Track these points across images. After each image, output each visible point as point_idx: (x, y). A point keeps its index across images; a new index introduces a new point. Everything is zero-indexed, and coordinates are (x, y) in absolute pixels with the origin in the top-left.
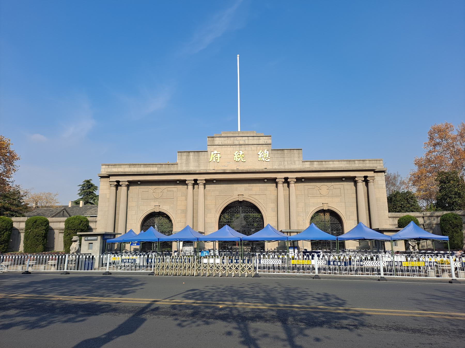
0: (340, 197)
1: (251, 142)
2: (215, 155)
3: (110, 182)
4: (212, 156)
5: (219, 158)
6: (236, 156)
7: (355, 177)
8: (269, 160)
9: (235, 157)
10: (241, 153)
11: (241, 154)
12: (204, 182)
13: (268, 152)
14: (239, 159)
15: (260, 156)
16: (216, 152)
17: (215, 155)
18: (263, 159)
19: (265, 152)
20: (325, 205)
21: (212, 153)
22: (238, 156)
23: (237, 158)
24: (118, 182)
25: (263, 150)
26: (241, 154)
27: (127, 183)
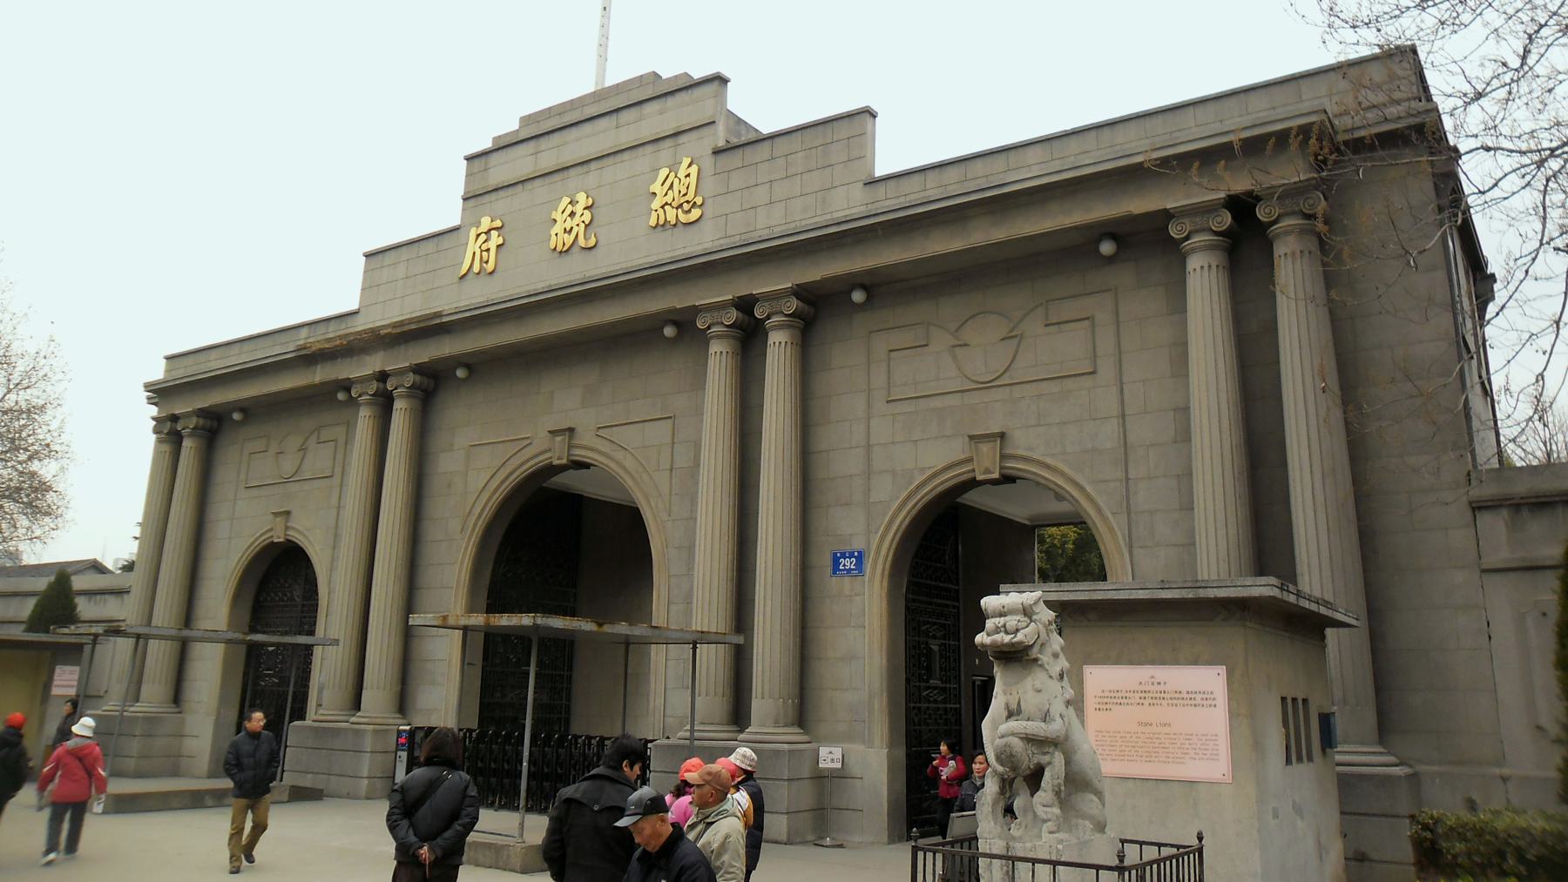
0: (1087, 382)
1: (626, 137)
2: (483, 237)
4: (473, 247)
6: (558, 228)
7: (1167, 215)
8: (696, 213)
10: (582, 199)
11: (579, 209)
13: (694, 170)
14: (569, 239)
16: (486, 223)
17: (483, 237)
18: (671, 214)
20: (985, 448)
21: (473, 233)
25: (674, 168)
26: (579, 209)
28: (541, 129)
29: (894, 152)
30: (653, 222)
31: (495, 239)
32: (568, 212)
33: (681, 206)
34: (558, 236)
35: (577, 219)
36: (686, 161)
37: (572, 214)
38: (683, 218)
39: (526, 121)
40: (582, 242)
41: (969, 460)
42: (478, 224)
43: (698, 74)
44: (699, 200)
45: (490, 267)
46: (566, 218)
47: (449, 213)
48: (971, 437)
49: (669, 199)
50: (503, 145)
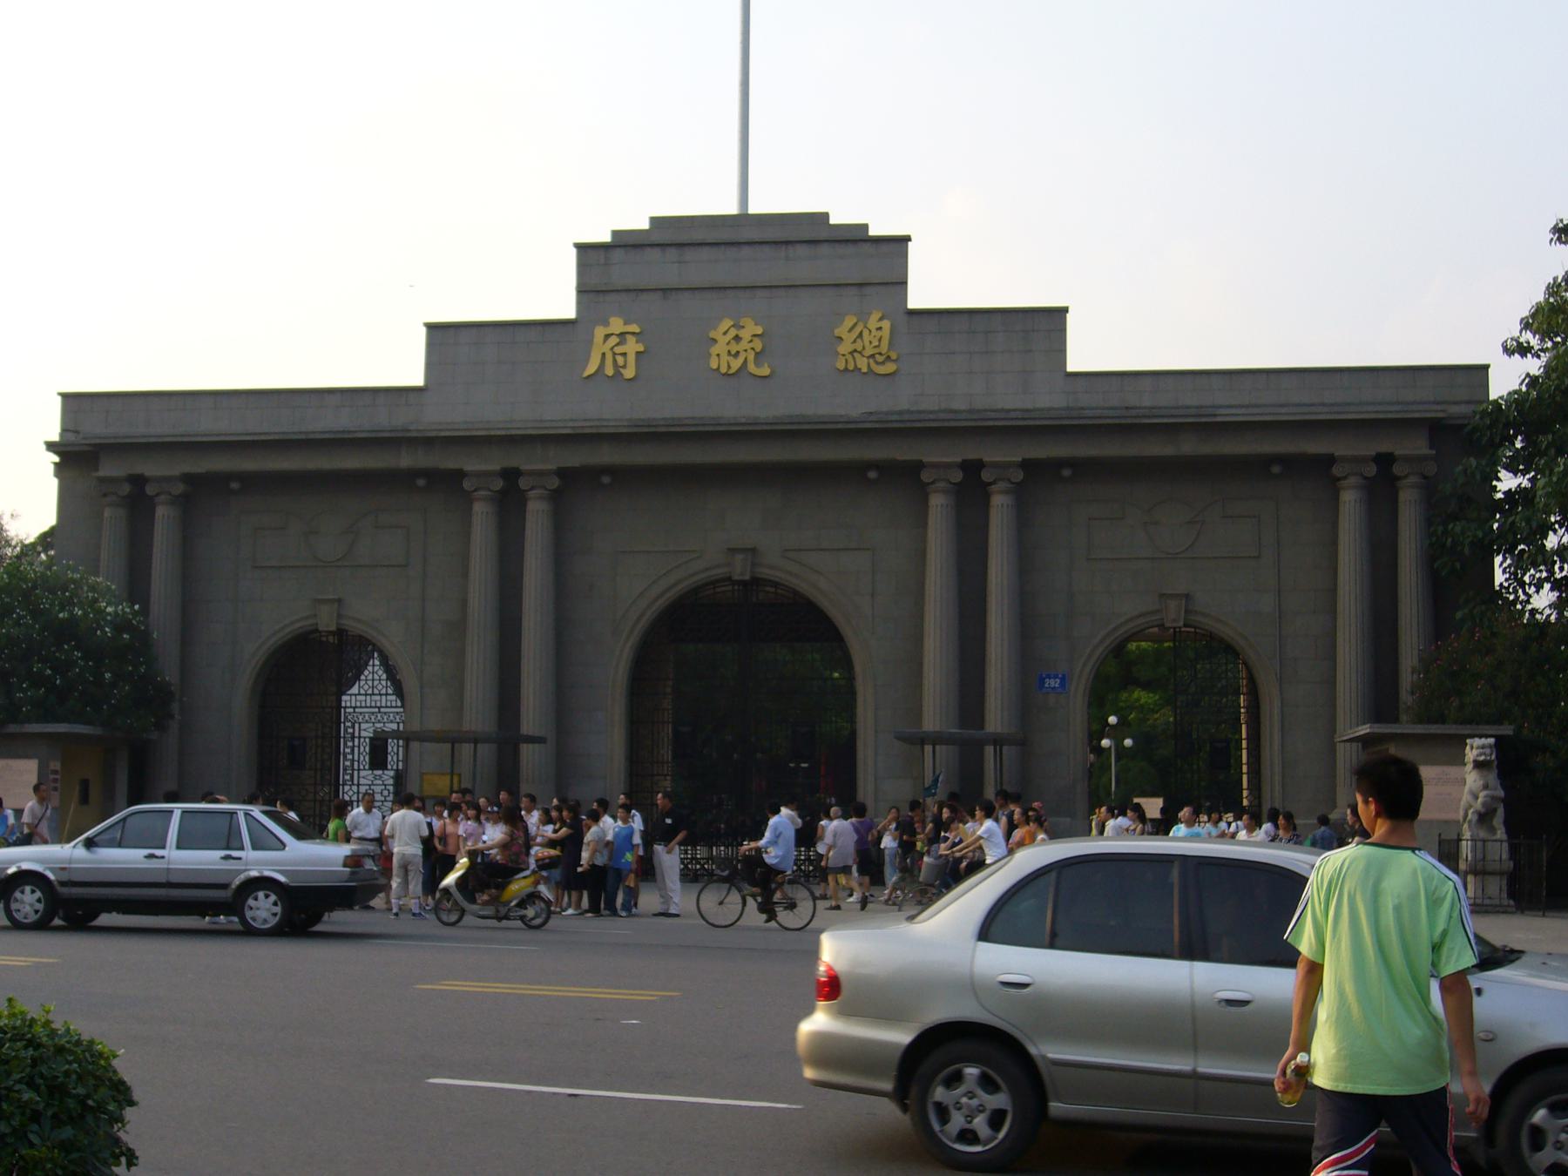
2: (614, 340)
3: (102, 480)
5: (631, 358)
8: (890, 368)
9: (714, 350)
12: (555, 483)
13: (886, 324)
14: (736, 364)
15: (844, 348)
16: (617, 325)
17: (614, 340)
18: (863, 364)
19: (873, 322)
21: (600, 332)
22: (734, 348)
23: (724, 358)
24: (138, 481)
25: (863, 317)
26: (746, 334)
27: (179, 488)
28: (674, 238)
29: (1089, 350)
30: (841, 366)
31: (632, 347)
32: (733, 332)
33: (872, 356)
34: (720, 357)
35: (744, 345)
36: (875, 316)
37: (737, 338)
38: (881, 370)
39: (656, 222)
40: (752, 368)
41: (1158, 611)
42: (606, 324)
43: (873, 232)
44: (894, 356)
45: (629, 373)
46: (732, 341)
47: (563, 305)
48: (1162, 596)
49: (859, 346)
50: (625, 242)
